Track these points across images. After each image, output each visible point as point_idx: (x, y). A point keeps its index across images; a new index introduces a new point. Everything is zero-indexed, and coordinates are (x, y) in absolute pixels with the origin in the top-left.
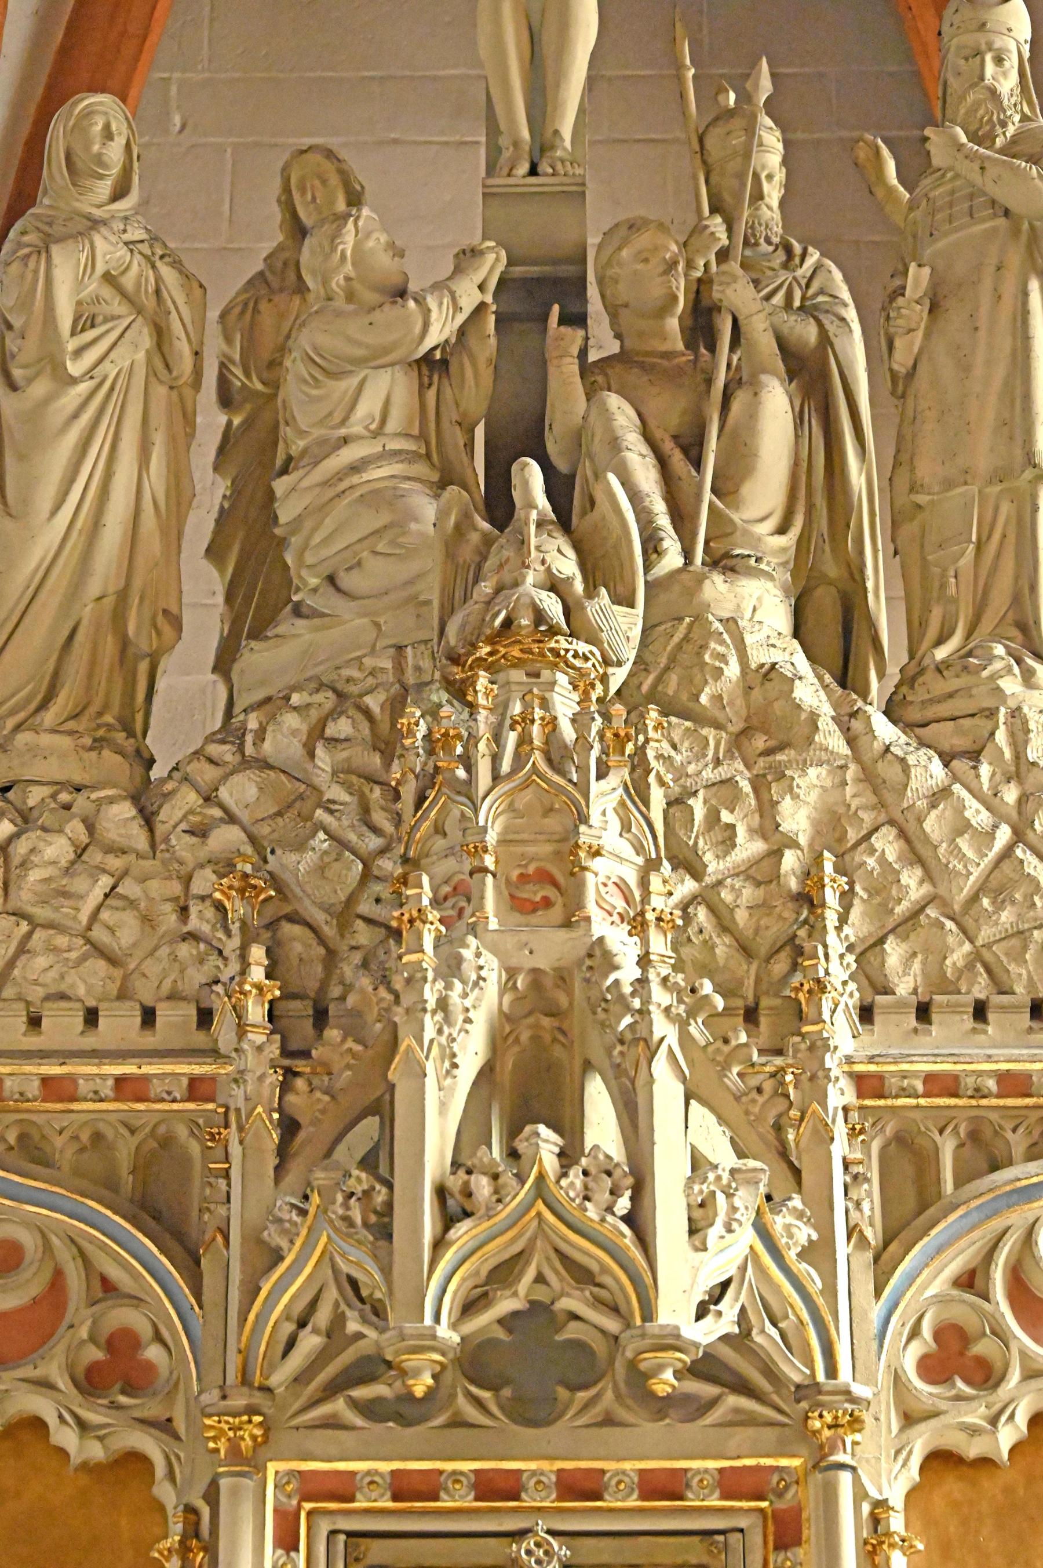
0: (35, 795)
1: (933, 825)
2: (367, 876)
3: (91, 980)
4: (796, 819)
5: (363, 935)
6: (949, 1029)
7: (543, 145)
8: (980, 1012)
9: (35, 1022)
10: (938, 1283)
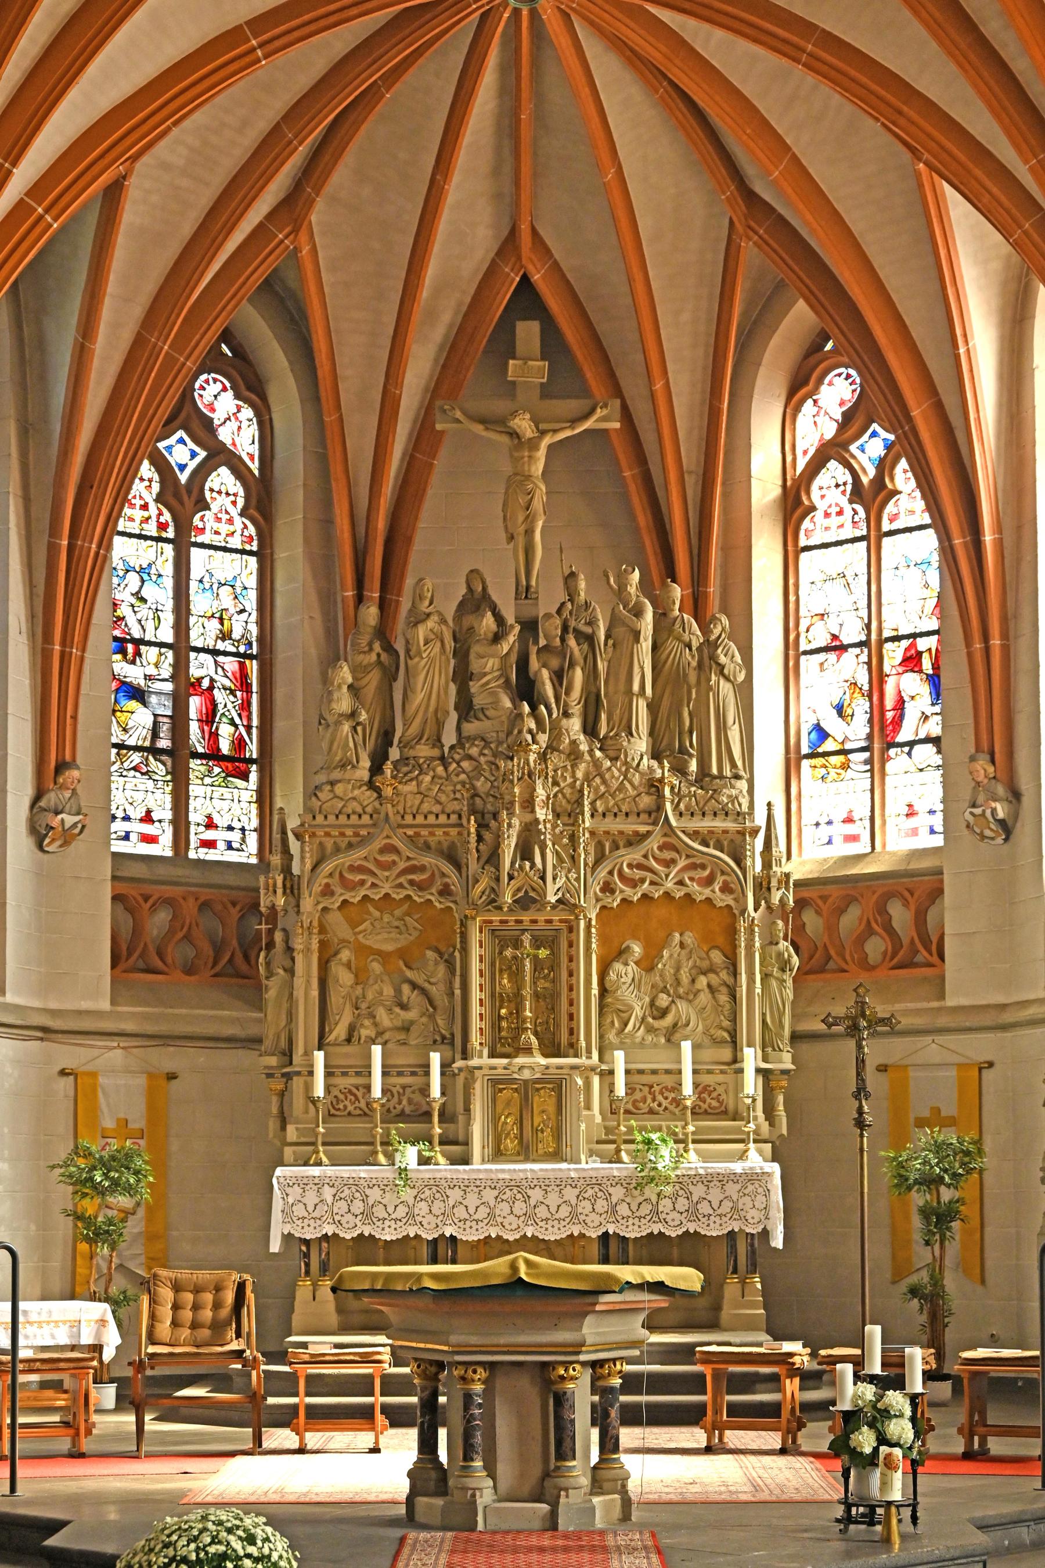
0: (421, 761)
1: (607, 776)
2: (492, 786)
3: (437, 809)
4: (580, 774)
5: (491, 799)
6: (609, 818)
7: (528, 588)
8: (615, 815)
9: (426, 817)
10: (604, 874)
